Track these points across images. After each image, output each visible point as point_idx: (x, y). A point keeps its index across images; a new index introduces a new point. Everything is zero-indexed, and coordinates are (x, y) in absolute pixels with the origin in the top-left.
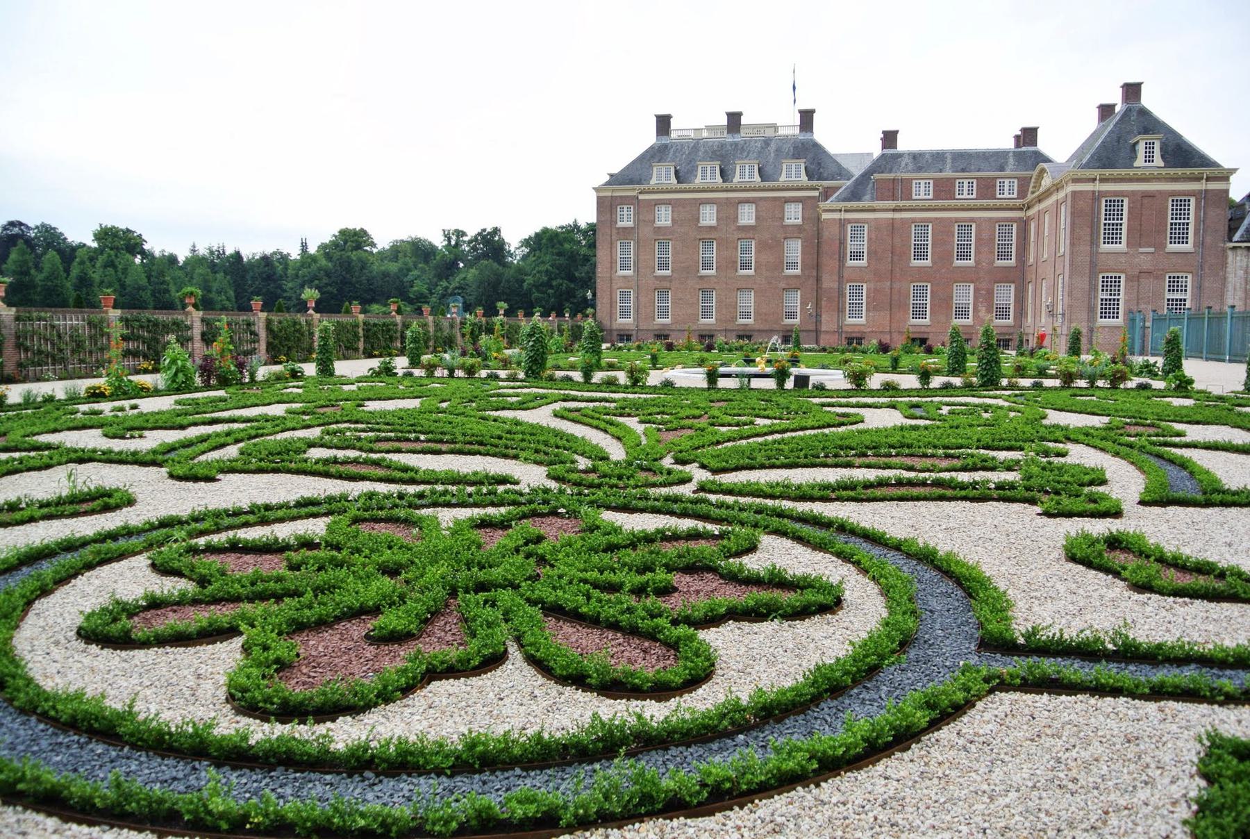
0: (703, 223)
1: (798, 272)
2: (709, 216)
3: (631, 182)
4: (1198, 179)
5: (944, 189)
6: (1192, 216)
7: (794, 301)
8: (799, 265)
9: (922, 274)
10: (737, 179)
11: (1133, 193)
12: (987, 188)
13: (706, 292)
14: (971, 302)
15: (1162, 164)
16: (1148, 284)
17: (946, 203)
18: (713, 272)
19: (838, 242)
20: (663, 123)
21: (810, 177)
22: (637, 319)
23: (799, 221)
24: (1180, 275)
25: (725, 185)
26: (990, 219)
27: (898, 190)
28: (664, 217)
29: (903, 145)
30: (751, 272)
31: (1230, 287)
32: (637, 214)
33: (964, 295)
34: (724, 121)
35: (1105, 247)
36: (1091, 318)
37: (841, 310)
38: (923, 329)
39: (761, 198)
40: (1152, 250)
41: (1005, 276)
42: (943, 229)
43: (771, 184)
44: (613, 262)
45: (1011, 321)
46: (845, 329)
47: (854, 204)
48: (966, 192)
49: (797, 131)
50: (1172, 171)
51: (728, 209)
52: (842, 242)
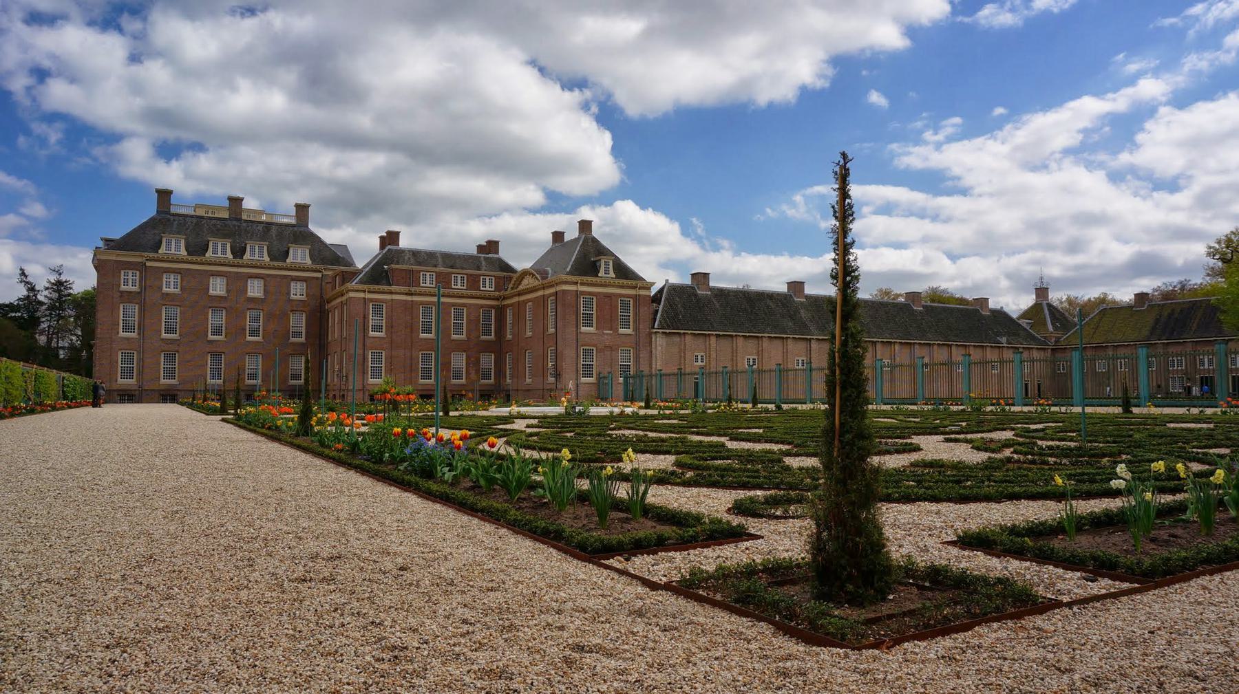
1: (303, 340)
2: (218, 287)
4: (635, 288)
5: (443, 280)
7: (298, 364)
9: (428, 344)
10: (247, 256)
12: (474, 282)
14: (464, 366)
15: (614, 276)
19: (362, 316)
25: (237, 261)
26: (478, 305)
28: (171, 285)
29: (404, 243)
33: (459, 361)
35: (584, 329)
37: (364, 373)
38: (429, 387)
39: (269, 275)
40: (611, 332)
41: (487, 347)
45: (492, 381)
46: (368, 387)
47: (372, 287)
50: (621, 281)
51: (237, 283)
52: (365, 317)
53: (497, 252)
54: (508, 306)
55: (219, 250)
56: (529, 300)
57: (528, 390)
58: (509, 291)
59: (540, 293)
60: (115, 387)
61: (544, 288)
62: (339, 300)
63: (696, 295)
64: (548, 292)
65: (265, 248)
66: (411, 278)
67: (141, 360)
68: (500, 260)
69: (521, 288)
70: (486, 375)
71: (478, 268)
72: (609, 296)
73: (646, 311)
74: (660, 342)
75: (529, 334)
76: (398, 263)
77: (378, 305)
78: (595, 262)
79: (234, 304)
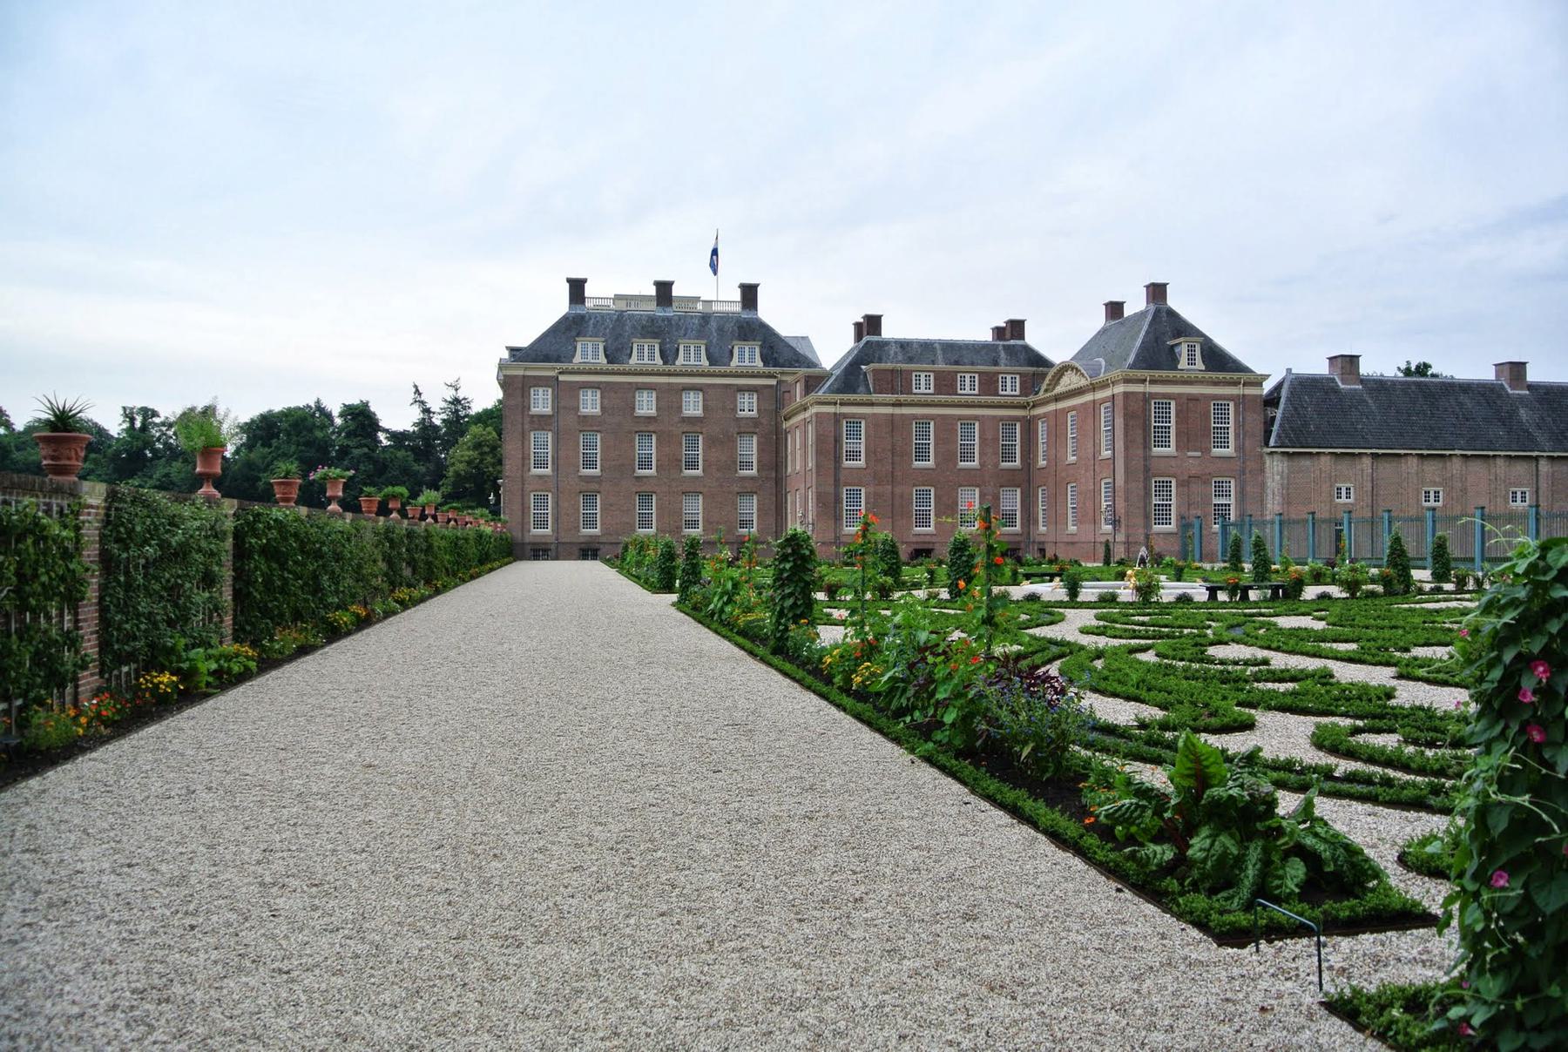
0: (534, 410)
1: (754, 472)
2: (646, 405)
3: (547, 359)
4: (1235, 383)
5: (946, 383)
6: (1232, 420)
7: (751, 507)
8: (755, 464)
9: (926, 477)
10: (680, 361)
11: (1180, 395)
12: (989, 384)
13: (645, 497)
15: (1203, 368)
16: (1196, 488)
17: (943, 398)
18: (653, 472)
20: (577, 288)
21: (766, 363)
22: (556, 530)
23: (754, 413)
24: (1224, 479)
25: (667, 368)
27: (896, 382)
28: (590, 404)
29: (889, 331)
30: (699, 472)
31: (1269, 491)
32: (556, 398)
34: (652, 291)
35: (1157, 451)
36: (1147, 526)
37: (837, 518)
38: (928, 539)
40: (1199, 454)
42: (945, 424)
43: (722, 369)
44: (525, 458)
45: (1018, 528)
47: (846, 397)
48: (967, 388)
49: (737, 308)
51: (670, 397)
52: (837, 440)
53: (1022, 337)
54: (1038, 417)
55: (644, 355)
56: (1073, 408)
57: (1073, 543)
58: (1041, 395)
59: (1088, 397)
60: (527, 540)
61: (1094, 390)
62: (800, 417)
63: (1336, 391)
64: (1100, 395)
65: (703, 348)
66: (896, 382)
67: (557, 504)
68: (1027, 349)
69: (1059, 389)
70: (1009, 519)
71: (996, 363)
72: (1193, 399)
73: (1255, 421)
74: (1275, 469)
75: (1072, 459)
76: (880, 361)
77: (854, 421)
78: (1173, 346)
79: (668, 425)
